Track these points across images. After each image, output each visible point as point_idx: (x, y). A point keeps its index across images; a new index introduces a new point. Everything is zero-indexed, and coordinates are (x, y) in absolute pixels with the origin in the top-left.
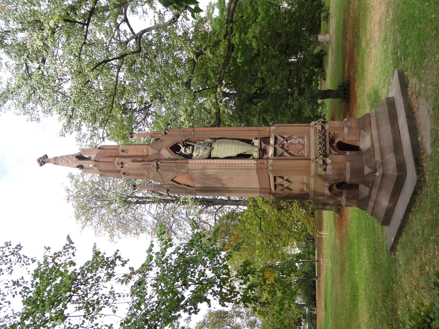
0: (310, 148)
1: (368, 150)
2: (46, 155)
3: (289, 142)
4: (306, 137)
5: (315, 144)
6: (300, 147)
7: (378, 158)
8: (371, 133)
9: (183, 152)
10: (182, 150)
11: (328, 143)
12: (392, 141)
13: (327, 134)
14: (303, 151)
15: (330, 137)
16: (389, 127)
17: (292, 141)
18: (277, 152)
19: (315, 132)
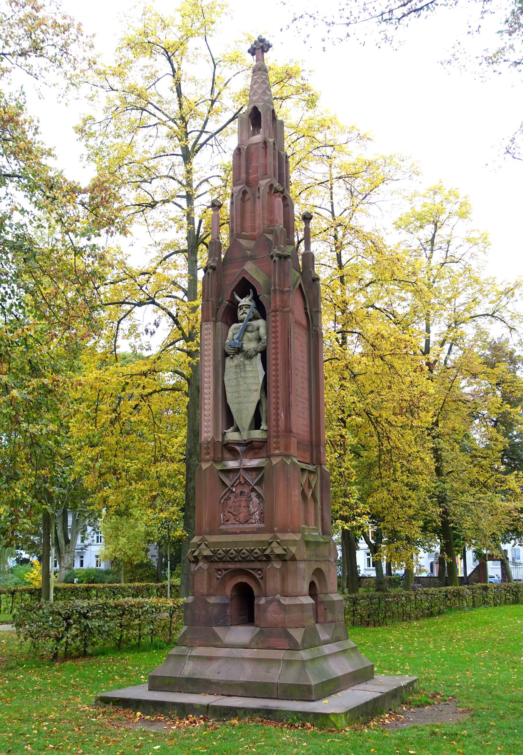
0: (236, 533)
1: (216, 637)
2: (269, 46)
3: (253, 495)
4: (262, 525)
5: (235, 543)
6: (242, 517)
7: (199, 651)
8: (252, 646)
9: (240, 305)
10: (245, 301)
11: (238, 566)
12: (210, 678)
13: (257, 565)
14: (234, 522)
15: (253, 569)
16: (242, 679)
17: (255, 500)
18: (231, 475)
19: (263, 542)
